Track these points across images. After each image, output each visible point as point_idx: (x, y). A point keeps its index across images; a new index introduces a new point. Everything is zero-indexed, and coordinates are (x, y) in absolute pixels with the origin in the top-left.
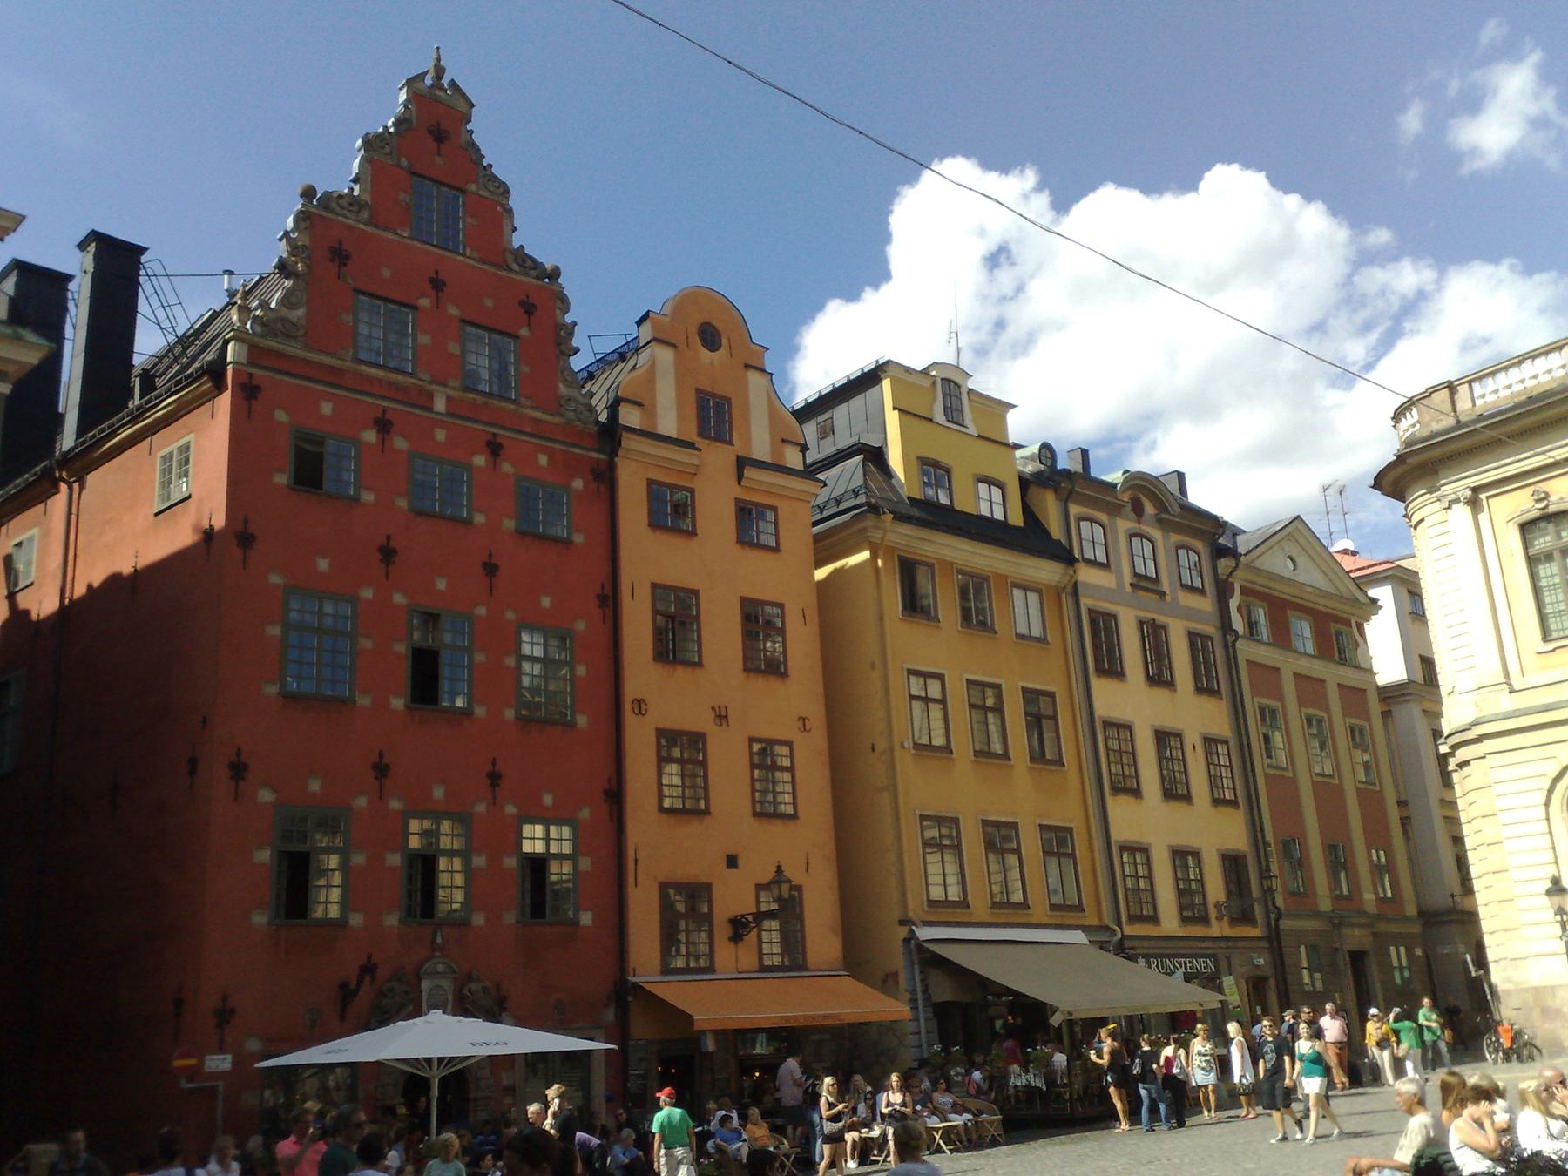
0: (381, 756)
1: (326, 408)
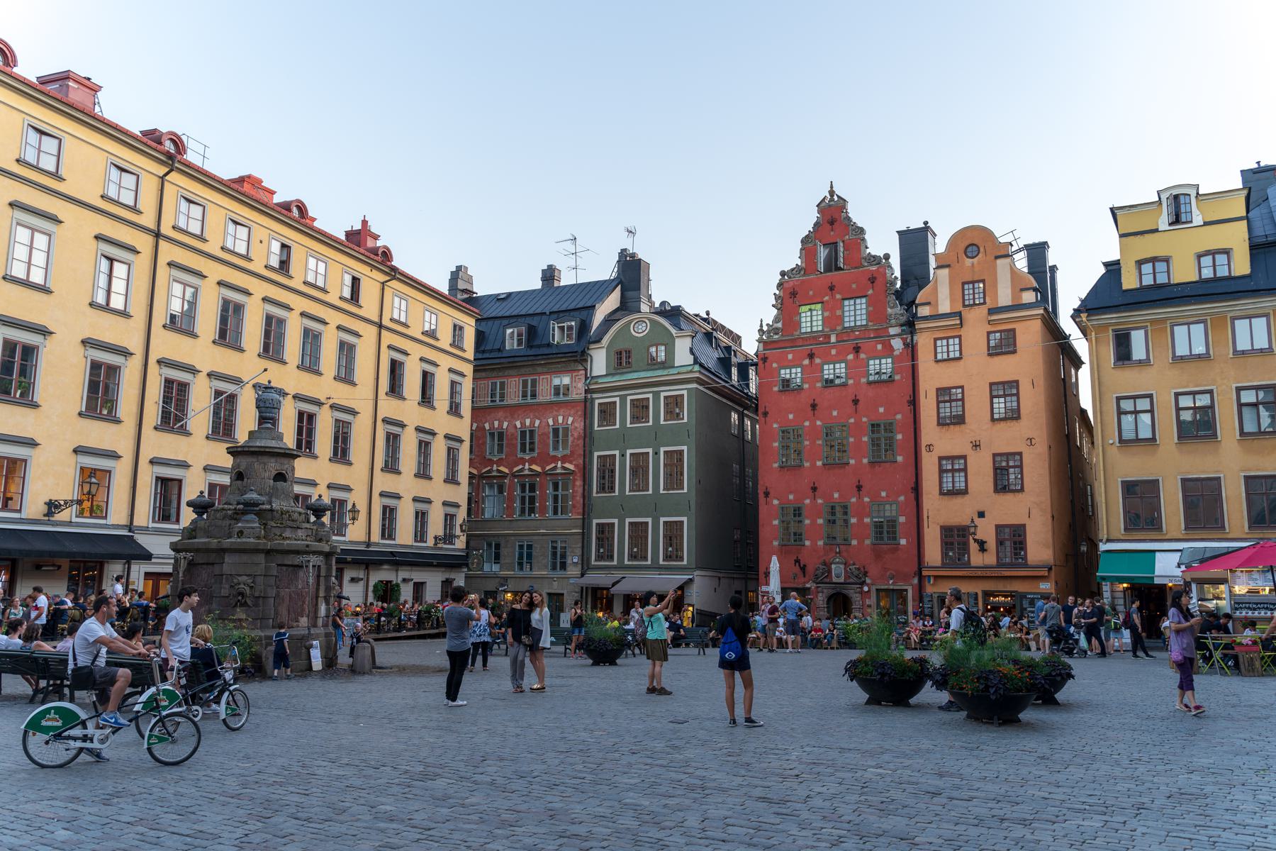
1: (790, 357)
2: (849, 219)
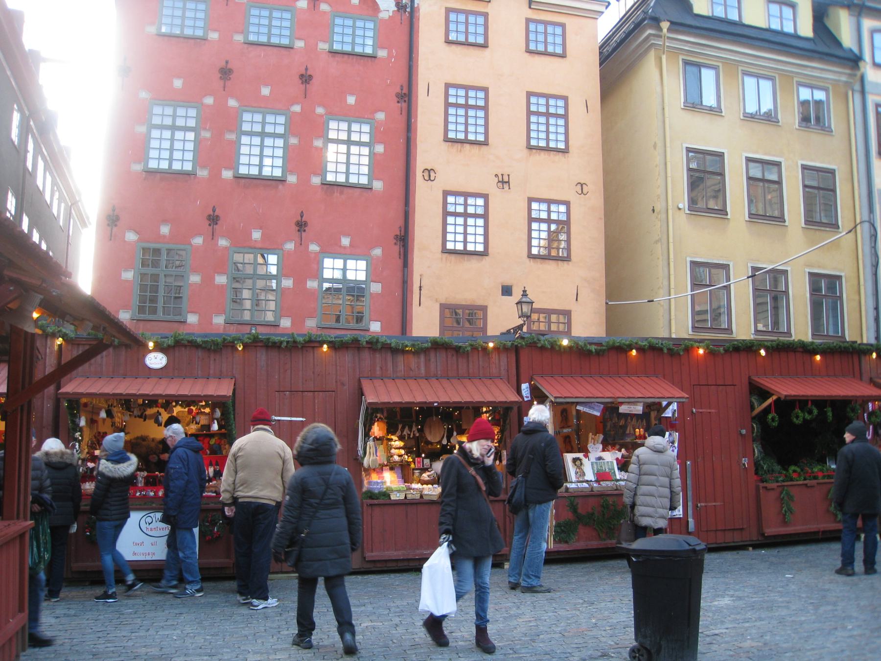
0: (214, 211)
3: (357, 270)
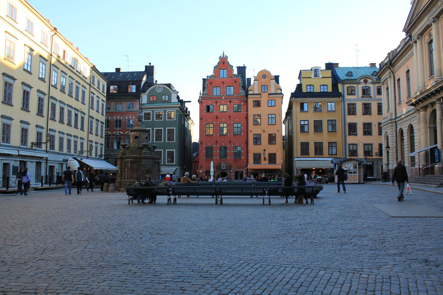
1: (210, 102)
2: (228, 62)
3: (239, 148)
